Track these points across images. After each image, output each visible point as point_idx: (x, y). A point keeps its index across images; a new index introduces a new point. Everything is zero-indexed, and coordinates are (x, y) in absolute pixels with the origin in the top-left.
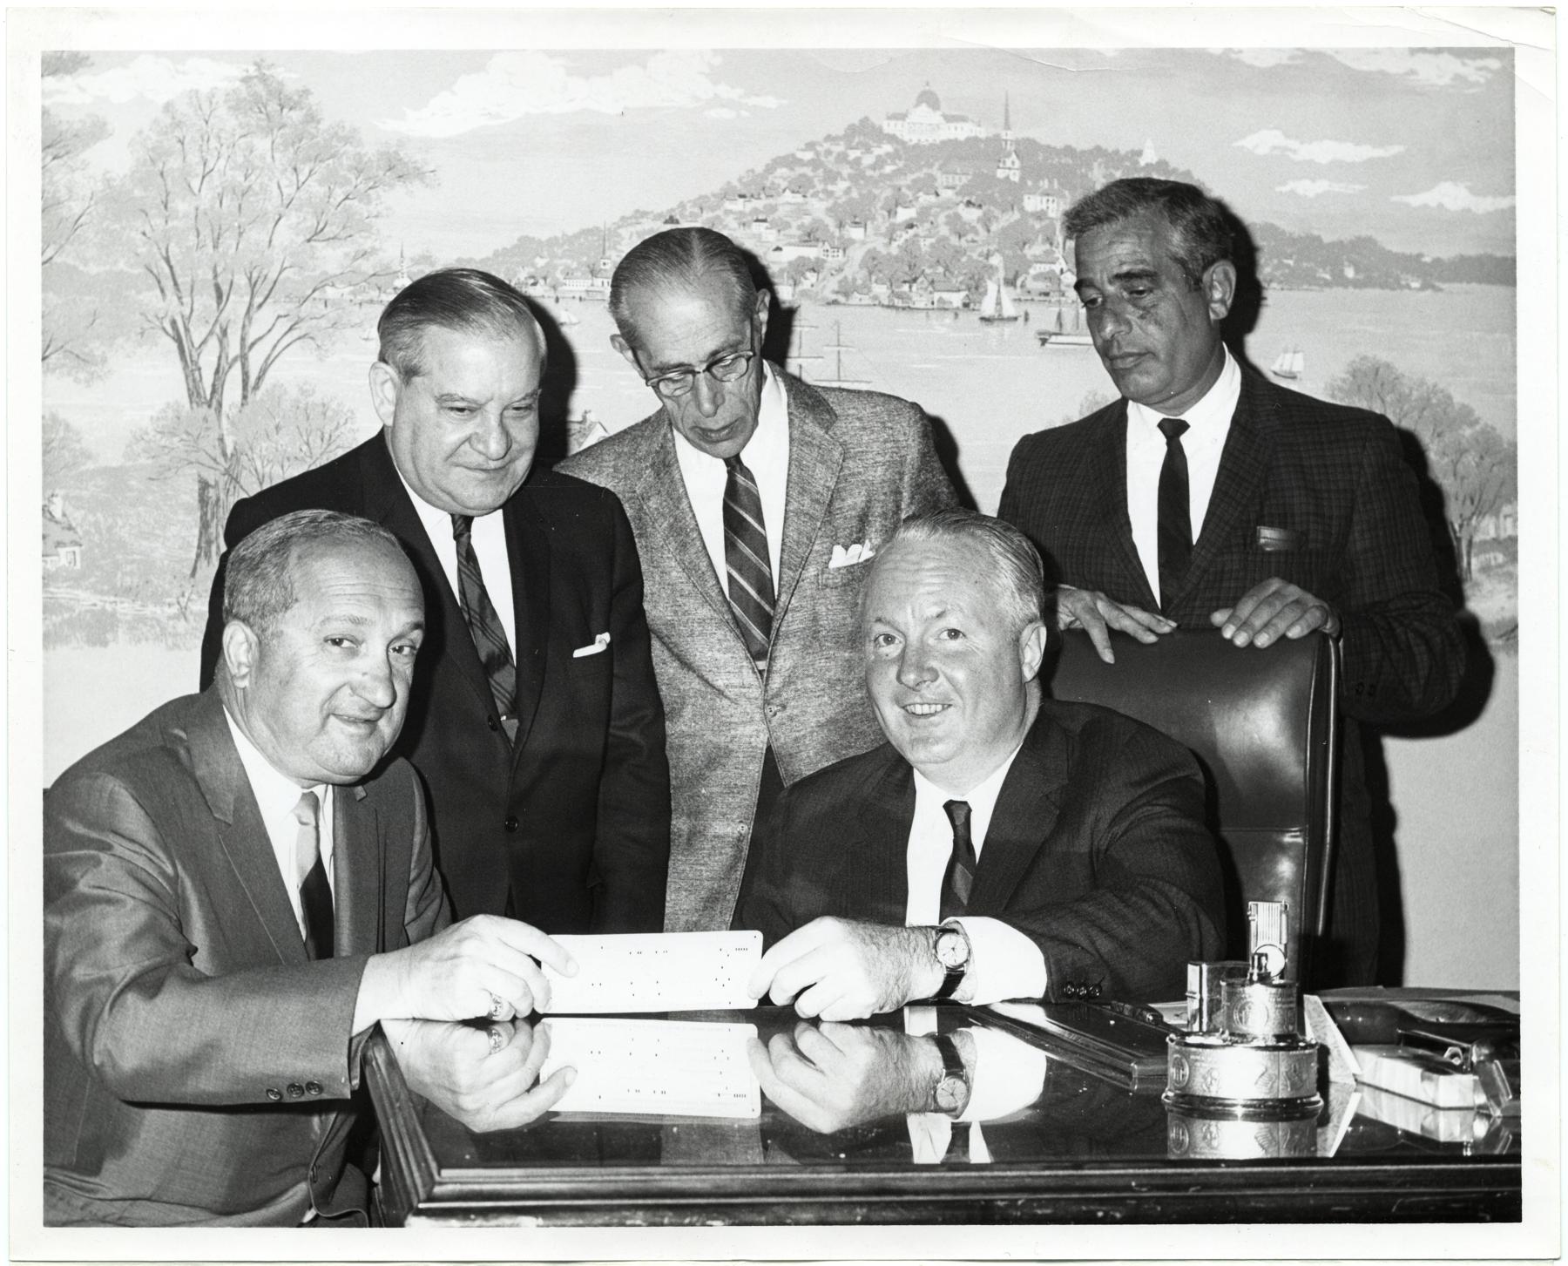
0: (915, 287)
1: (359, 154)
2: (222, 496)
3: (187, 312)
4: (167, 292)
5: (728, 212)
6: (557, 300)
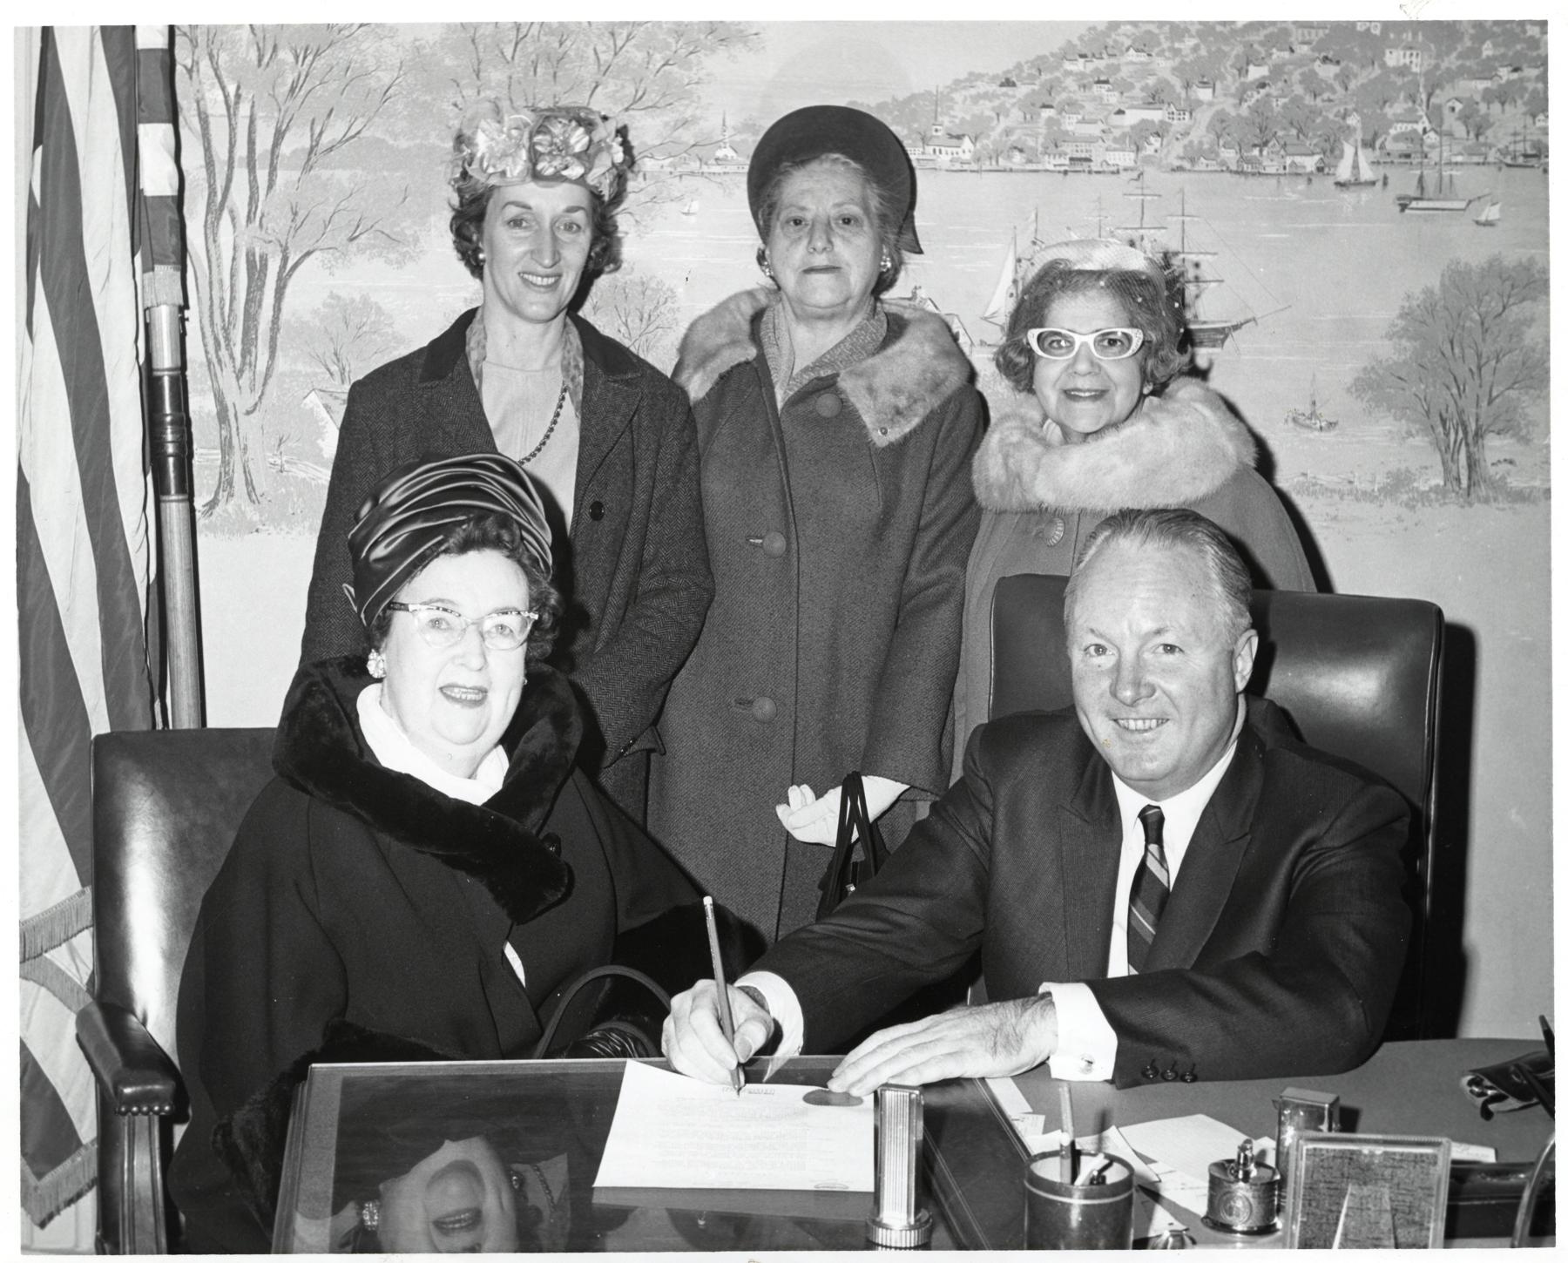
0: (1265, 153)
5: (1069, 73)
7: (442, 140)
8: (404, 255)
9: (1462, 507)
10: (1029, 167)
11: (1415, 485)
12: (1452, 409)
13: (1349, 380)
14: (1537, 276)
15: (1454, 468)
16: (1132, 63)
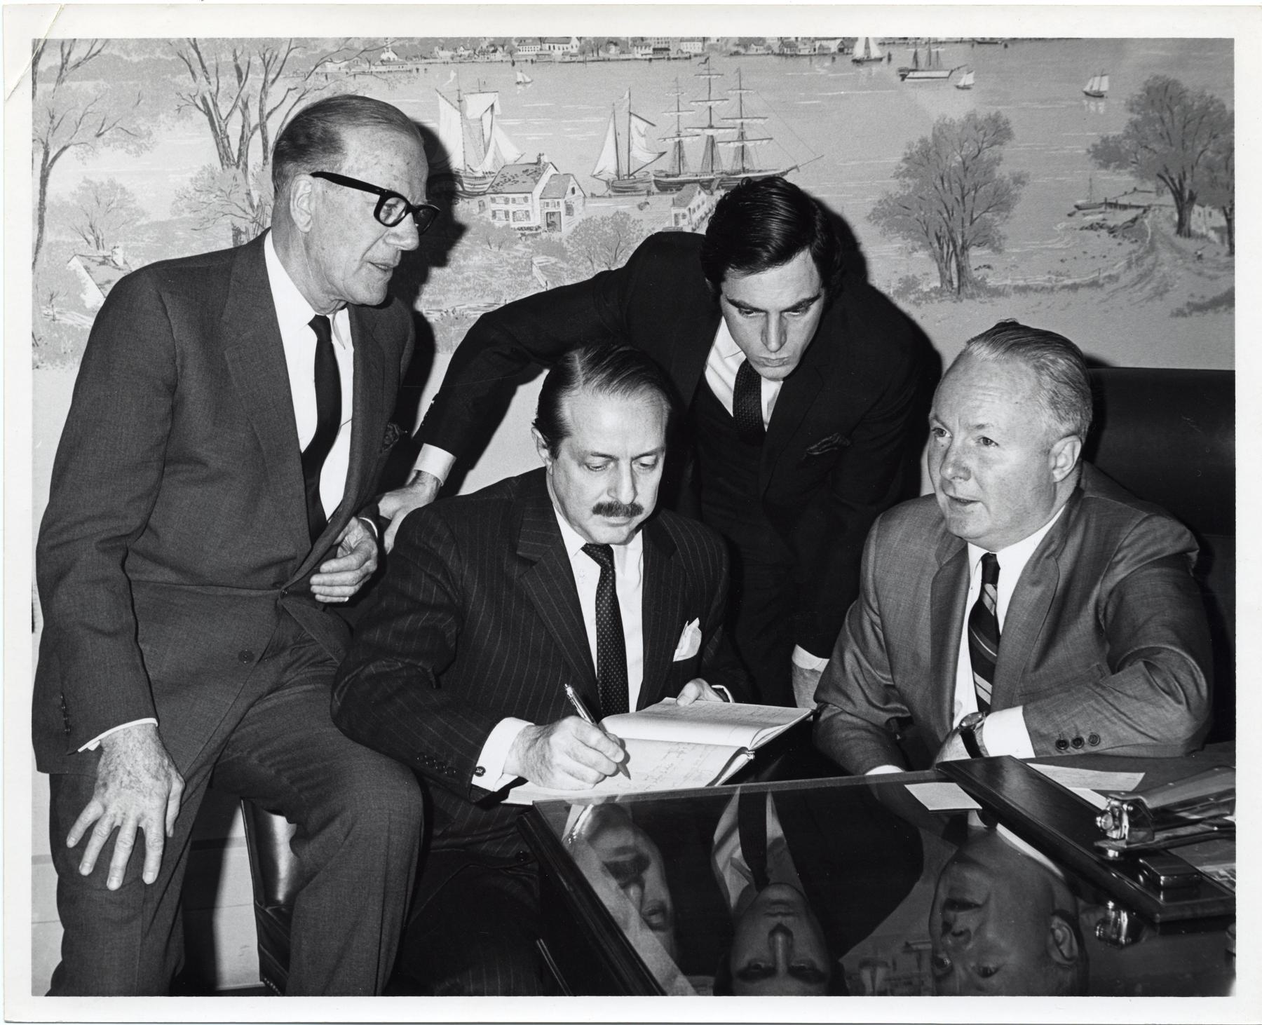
3: (215, 89)
4: (198, 75)
6: (513, 64)
7: (166, 54)
8: (140, 146)
9: (955, 302)
11: (920, 287)
12: (944, 229)
13: (870, 211)
15: (948, 273)
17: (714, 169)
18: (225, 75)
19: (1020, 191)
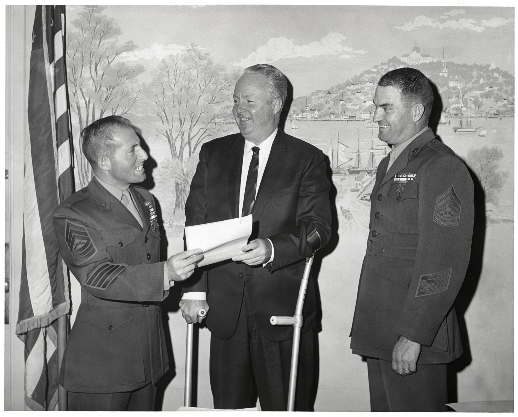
1: (225, 74)
2: (183, 188)
4: (164, 122)
5: (348, 90)
6: (291, 121)
7: (153, 114)
10: (336, 119)
14: (499, 152)
16: (368, 86)
17: (373, 166)
18: (175, 123)
19: (506, 180)
